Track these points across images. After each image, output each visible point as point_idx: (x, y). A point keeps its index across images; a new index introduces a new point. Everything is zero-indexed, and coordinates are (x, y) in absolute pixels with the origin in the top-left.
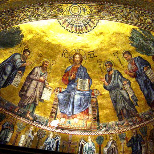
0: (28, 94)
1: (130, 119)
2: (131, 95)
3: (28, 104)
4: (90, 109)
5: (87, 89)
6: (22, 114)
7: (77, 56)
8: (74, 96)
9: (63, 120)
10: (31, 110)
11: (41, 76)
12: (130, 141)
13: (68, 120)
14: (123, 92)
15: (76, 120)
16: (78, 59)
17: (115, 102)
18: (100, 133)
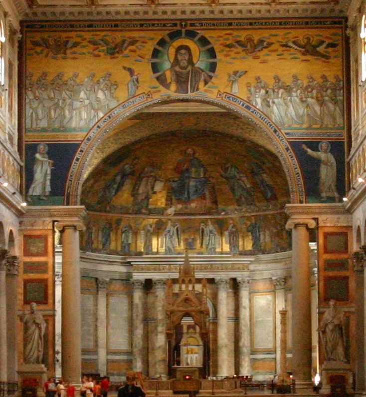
0: (140, 191)
1: (248, 207)
2: (248, 186)
3: (141, 201)
4: (207, 193)
5: (202, 176)
6: (137, 211)
7: (190, 150)
8: (189, 184)
9: (180, 206)
10: (144, 205)
11: (151, 172)
12: (250, 226)
13: (184, 206)
14: (242, 183)
15: (193, 205)
16: (192, 152)
17: (233, 189)
18: (220, 217)
